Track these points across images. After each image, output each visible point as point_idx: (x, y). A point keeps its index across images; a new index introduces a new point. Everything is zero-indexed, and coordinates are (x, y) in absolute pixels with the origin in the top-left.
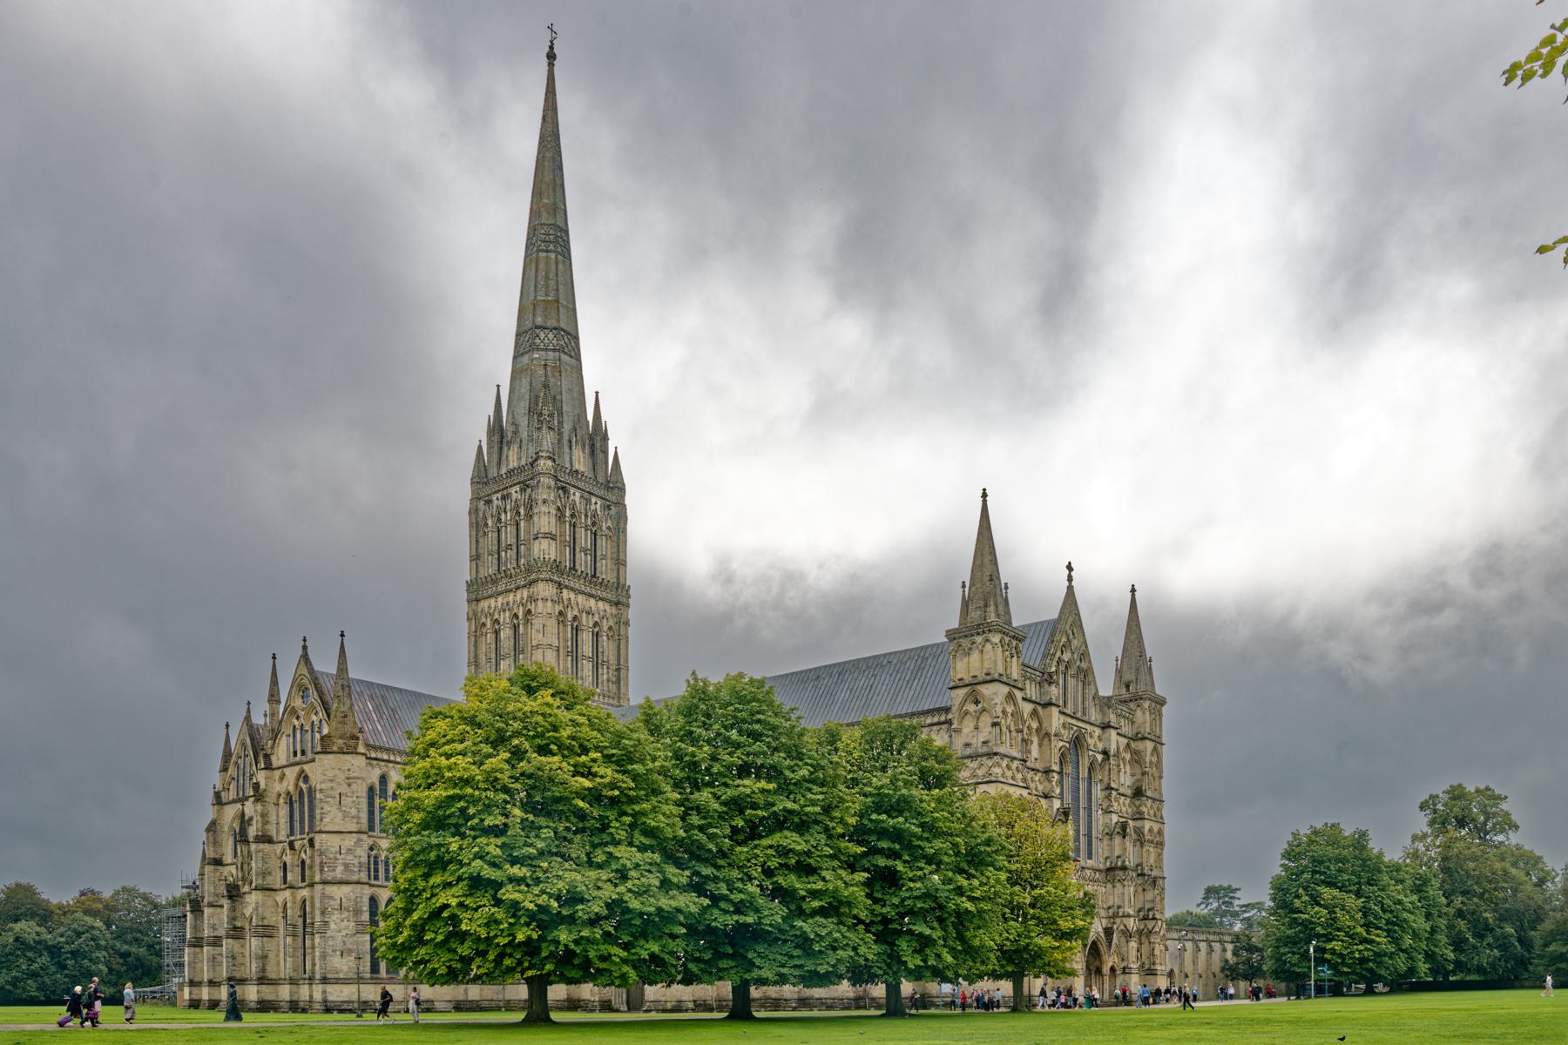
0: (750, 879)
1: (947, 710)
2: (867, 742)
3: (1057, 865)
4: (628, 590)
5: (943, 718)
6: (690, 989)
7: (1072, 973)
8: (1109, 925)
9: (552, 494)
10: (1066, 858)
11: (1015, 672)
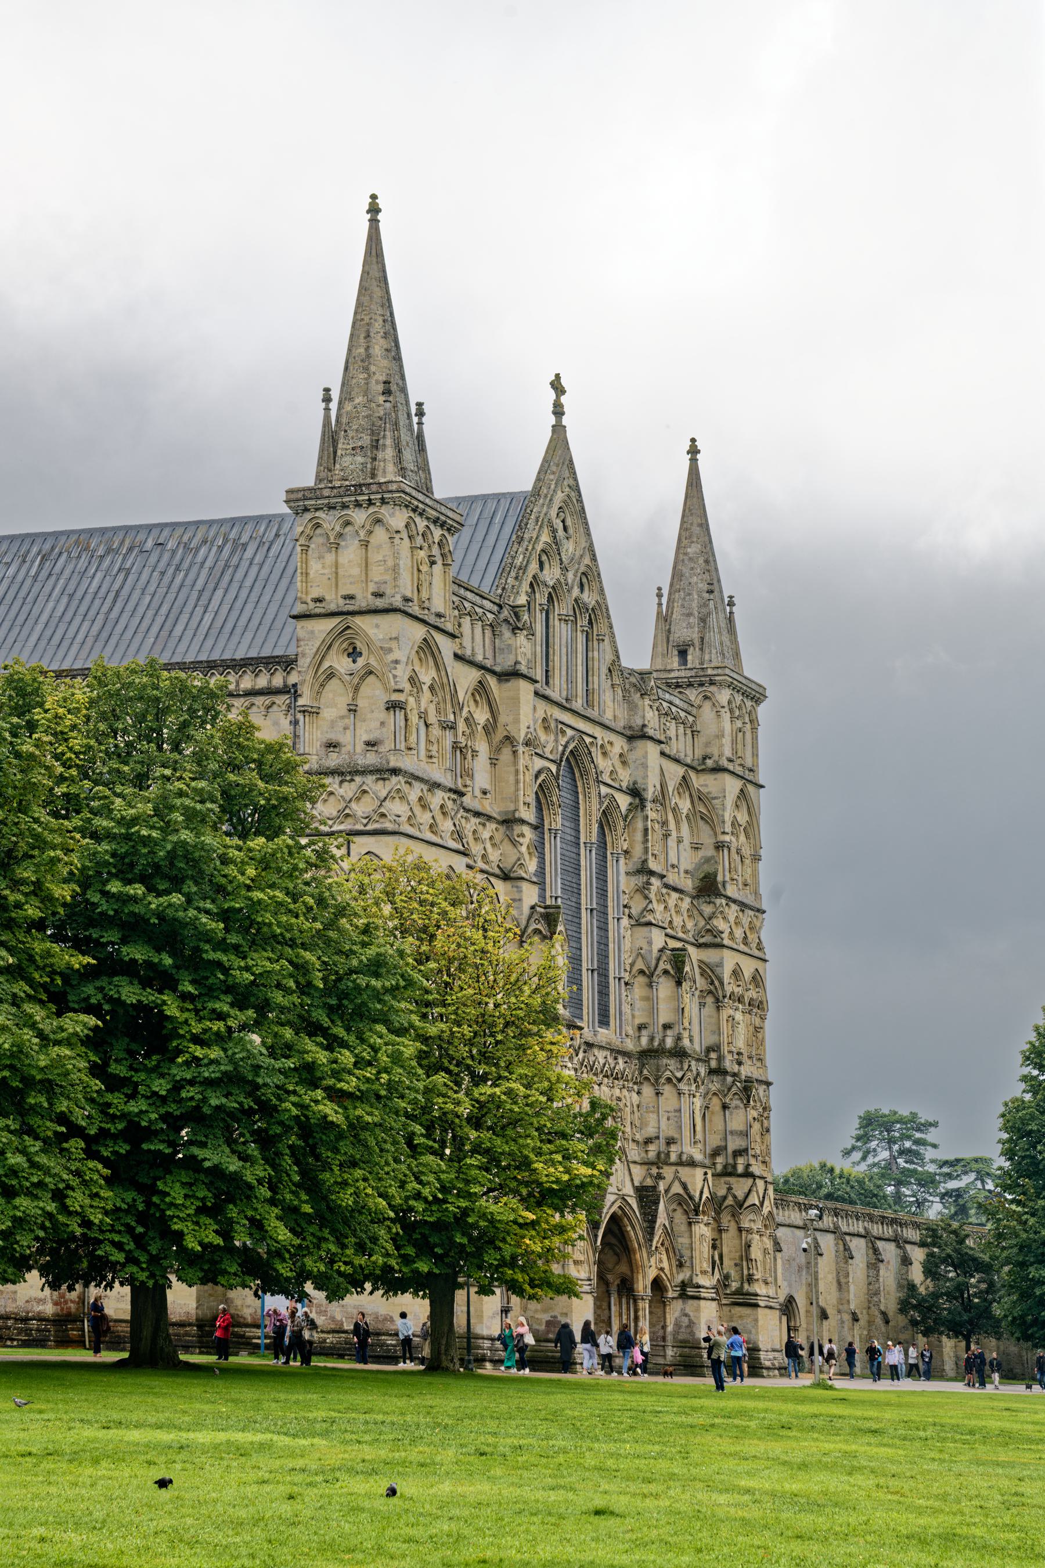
1: (288, 663)
2: (103, 717)
3: (529, 1034)
5: (278, 681)
7: (567, 1288)
8: (649, 1182)
10: (551, 1019)
11: (439, 598)
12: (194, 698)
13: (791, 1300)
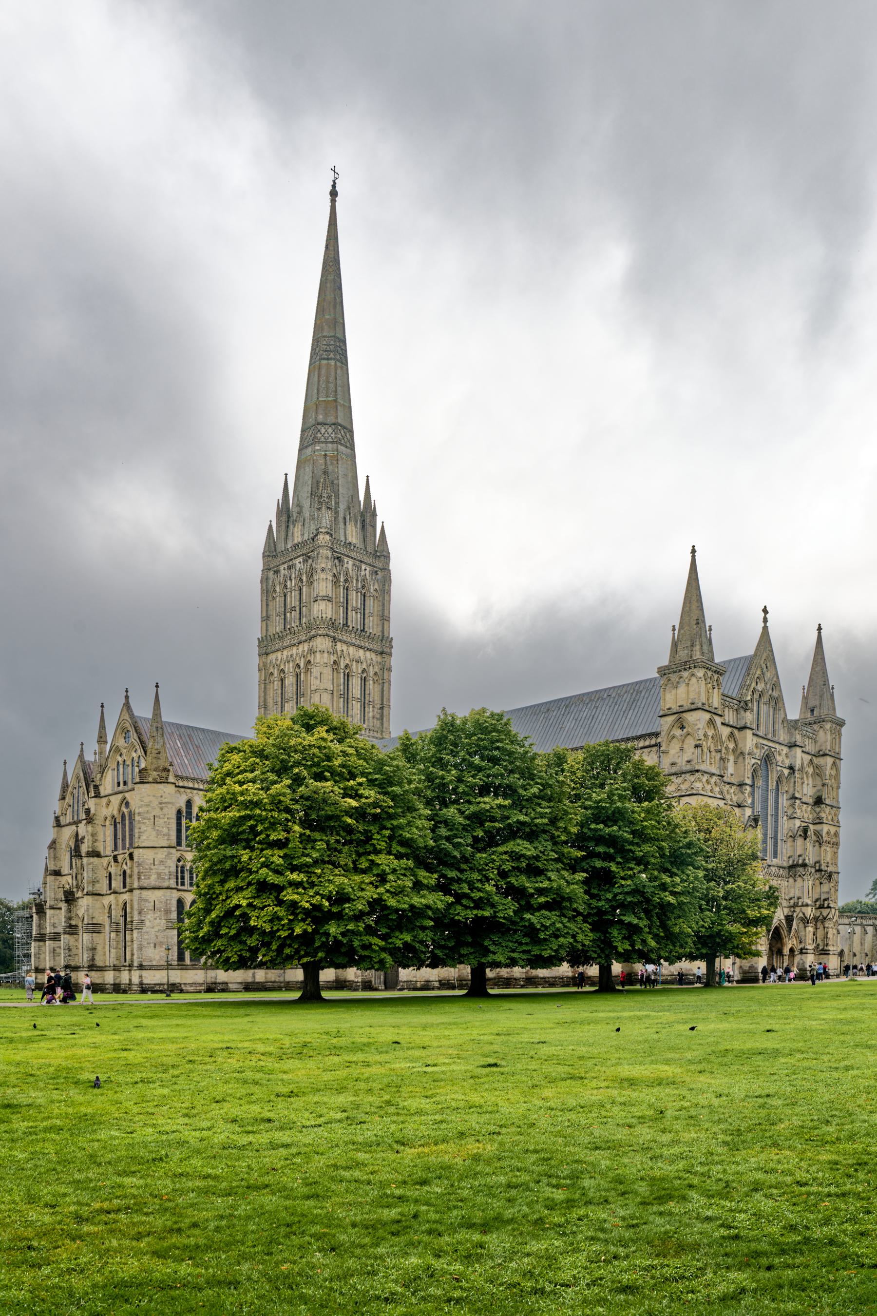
0: (488, 880)
1: (657, 735)
2: (589, 764)
4: (391, 642)
5: (653, 742)
6: (436, 971)
7: (757, 954)
8: (790, 914)
9: (329, 564)
10: (754, 857)
11: (716, 702)
12: (622, 753)
13: (842, 951)
